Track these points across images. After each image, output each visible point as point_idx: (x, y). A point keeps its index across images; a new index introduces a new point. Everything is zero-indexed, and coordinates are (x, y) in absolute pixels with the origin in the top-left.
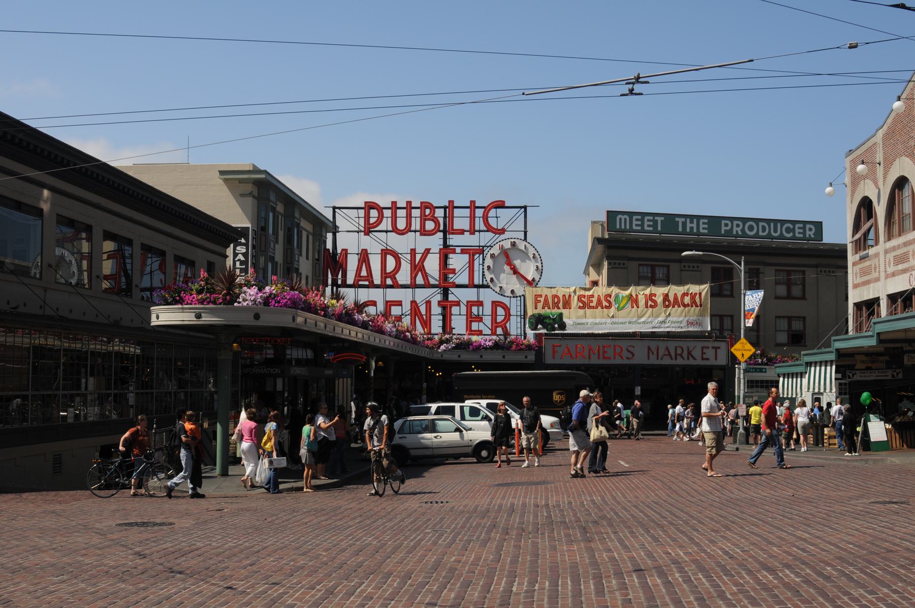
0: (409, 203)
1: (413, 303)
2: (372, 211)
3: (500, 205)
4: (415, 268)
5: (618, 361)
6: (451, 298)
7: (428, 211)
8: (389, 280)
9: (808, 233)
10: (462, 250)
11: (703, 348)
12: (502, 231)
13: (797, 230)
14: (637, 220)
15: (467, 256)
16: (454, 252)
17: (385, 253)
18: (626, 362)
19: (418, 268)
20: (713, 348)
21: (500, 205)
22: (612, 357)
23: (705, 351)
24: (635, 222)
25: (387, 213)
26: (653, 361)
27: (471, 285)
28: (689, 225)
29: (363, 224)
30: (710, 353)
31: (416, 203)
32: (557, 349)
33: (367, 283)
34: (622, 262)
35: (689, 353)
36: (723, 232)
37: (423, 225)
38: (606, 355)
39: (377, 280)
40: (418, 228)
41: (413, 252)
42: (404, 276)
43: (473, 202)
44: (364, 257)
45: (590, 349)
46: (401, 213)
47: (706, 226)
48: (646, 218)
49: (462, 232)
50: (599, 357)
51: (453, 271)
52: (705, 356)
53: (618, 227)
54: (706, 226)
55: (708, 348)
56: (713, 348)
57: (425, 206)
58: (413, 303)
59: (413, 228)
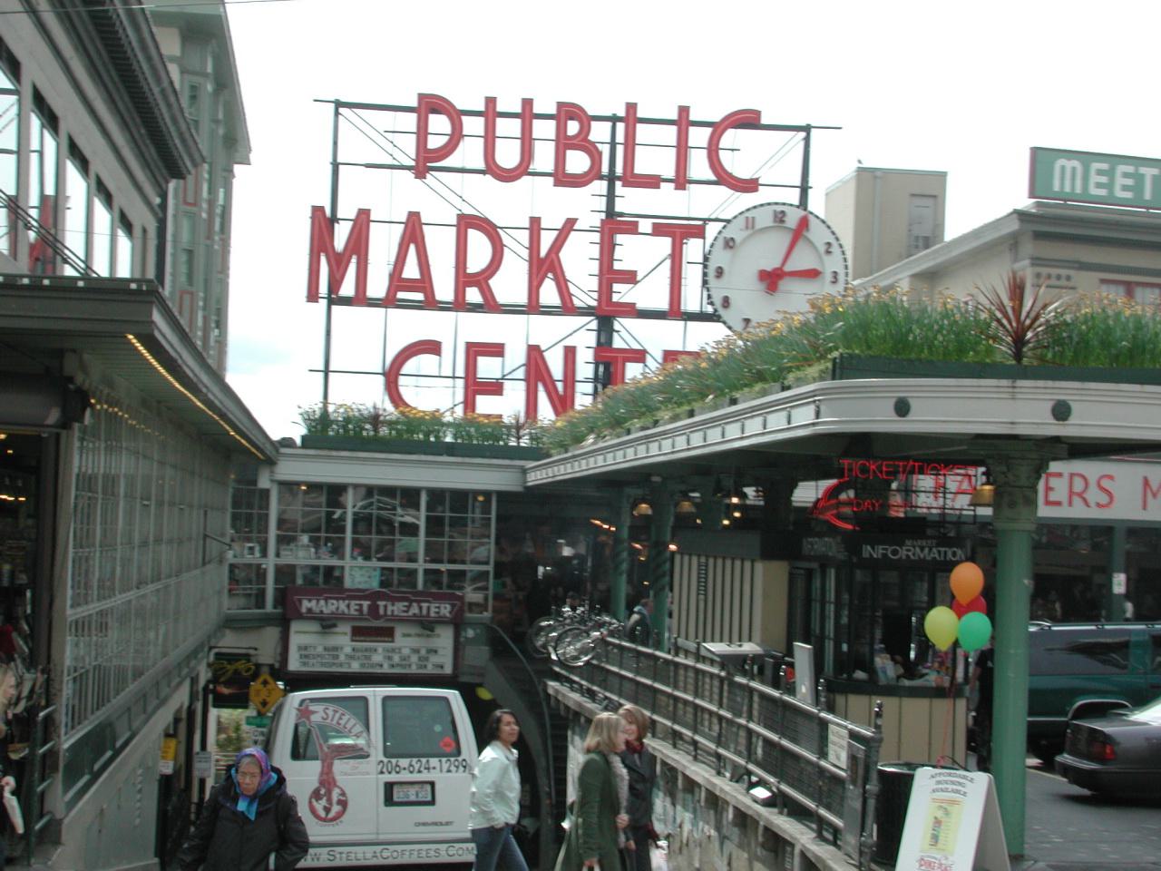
0: (527, 103)
1: (535, 354)
2: (433, 118)
3: (748, 120)
4: (539, 270)
5: (1078, 512)
6: (618, 343)
7: (573, 128)
8: (475, 290)
10: (654, 224)
12: (750, 186)
14: (1100, 172)
15: (665, 244)
16: (632, 229)
17: (466, 223)
19: (544, 266)
21: (748, 120)
22: (1064, 499)
24: (1094, 178)
25: (473, 126)
27: (675, 312)
29: (412, 152)
31: (545, 105)
33: (419, 296)
34: (1064, 272)
37: (560, 159)
38: (1053, 497)
39: (444, 291)
40: (550, 168)
41: (535, 225)
42: (511, 283)
43: (684, 111)
44: (413, 231)
46: (508, 128)
48: (1122, 168)
49: (653, 182)
51: (630, 277)
53: (1056, 187)
57: (568, 111)
58: (535, 354)
59: (537, 165)
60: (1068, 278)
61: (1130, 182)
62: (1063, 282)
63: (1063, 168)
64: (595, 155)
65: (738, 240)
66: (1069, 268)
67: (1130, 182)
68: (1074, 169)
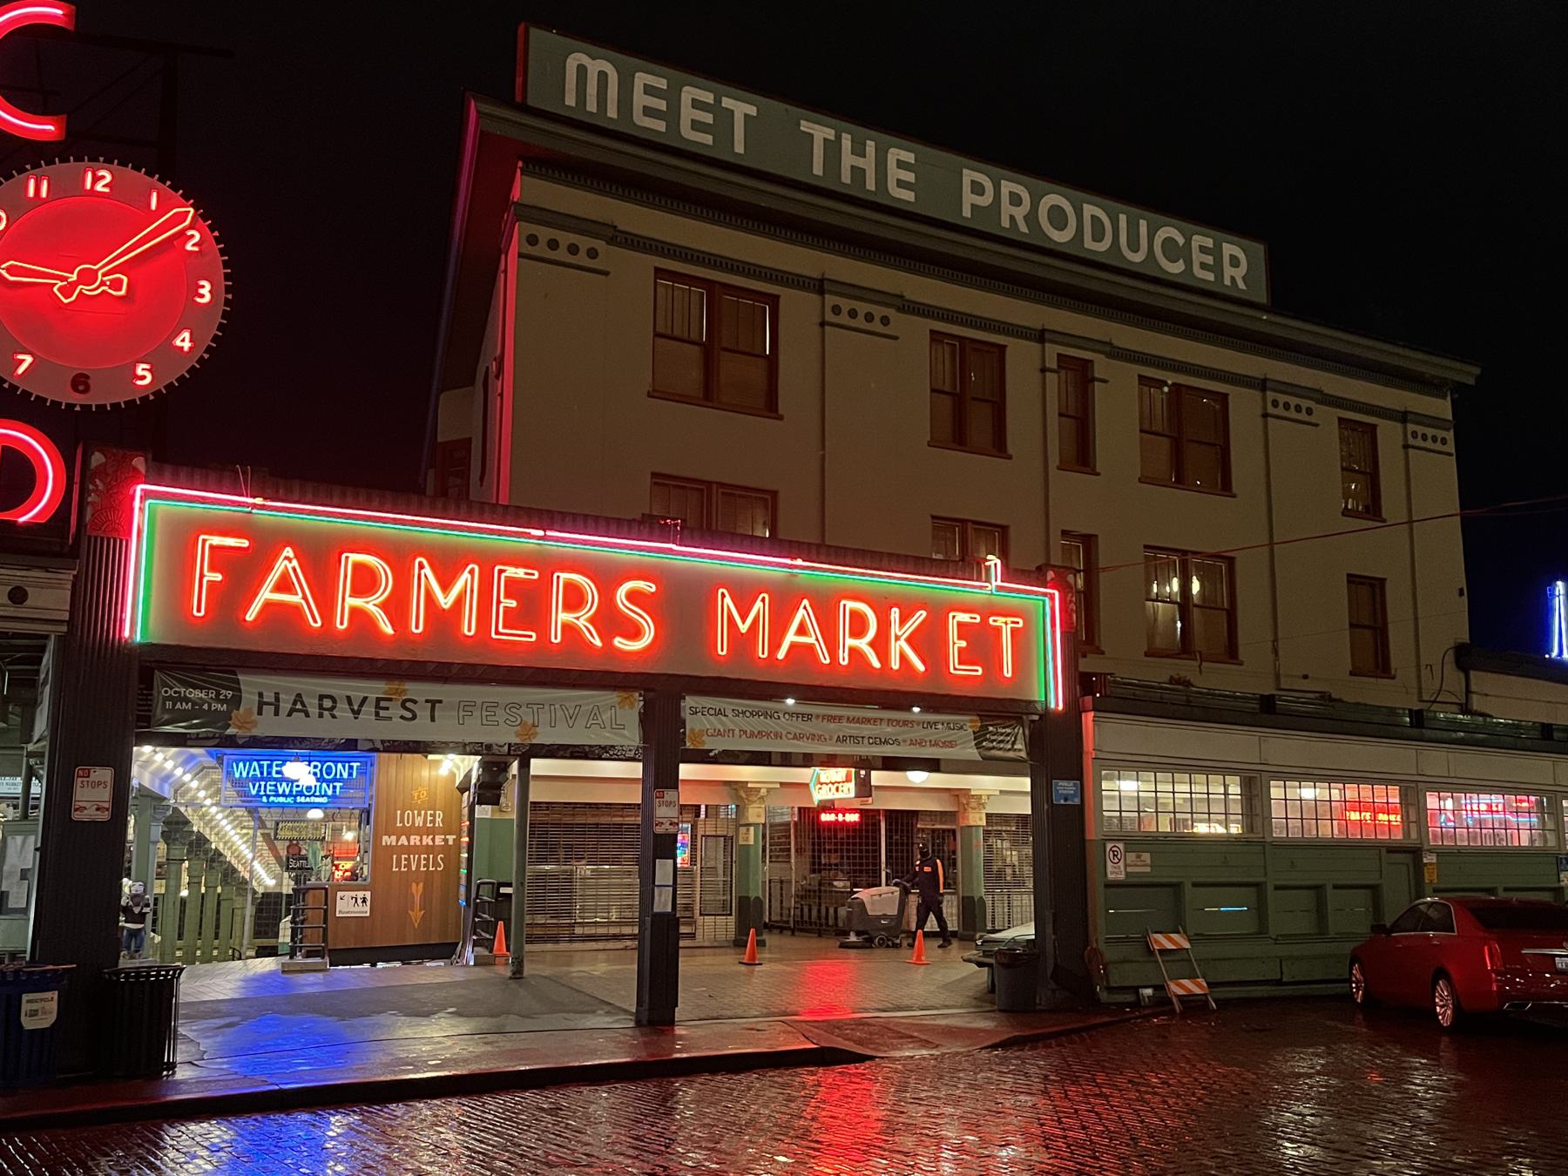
9: (1229, 271)
13: (1197, 257)
24: (640, 100)
28: (848, 160)
36: (967, 213)
47: (910, 177)
53: (570, 101)
54: (910, 177)
60: (593, 254)
61: (708, 118)
66: (597, 236)
67: (708, 118)
68: (603, 76)
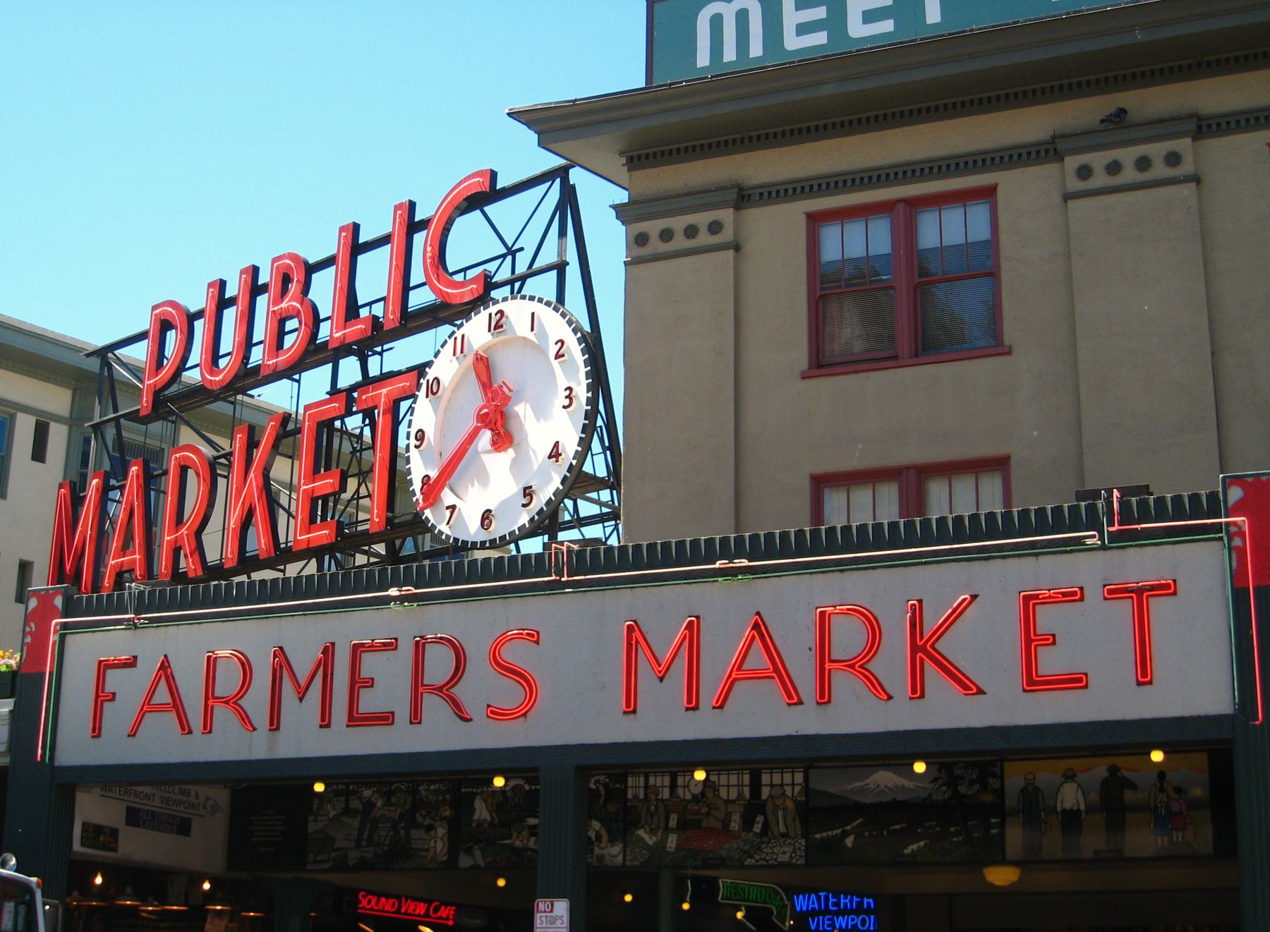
5: (438, 733)
11: (1030, 602)
18: (486, 735)
20: (1115, 593)
23: (1046, 618)
26: (663, 719)
30: (1090, 638)
32: (114, 679)
34: (702, 219)
35: (924, 649)
38: (369, 702)
45: (282, 662)
50: (325, 722)
52: (1050, 662)
53: (703, 60)
55: (1077, 596)
56: (1115, 593)
62: (704, 238)
63: (717, 21)
64: (316, 320)
65: (445, 381)
